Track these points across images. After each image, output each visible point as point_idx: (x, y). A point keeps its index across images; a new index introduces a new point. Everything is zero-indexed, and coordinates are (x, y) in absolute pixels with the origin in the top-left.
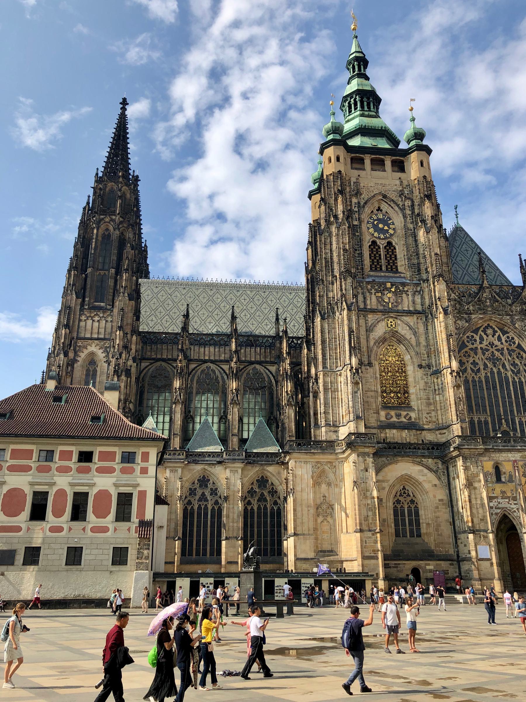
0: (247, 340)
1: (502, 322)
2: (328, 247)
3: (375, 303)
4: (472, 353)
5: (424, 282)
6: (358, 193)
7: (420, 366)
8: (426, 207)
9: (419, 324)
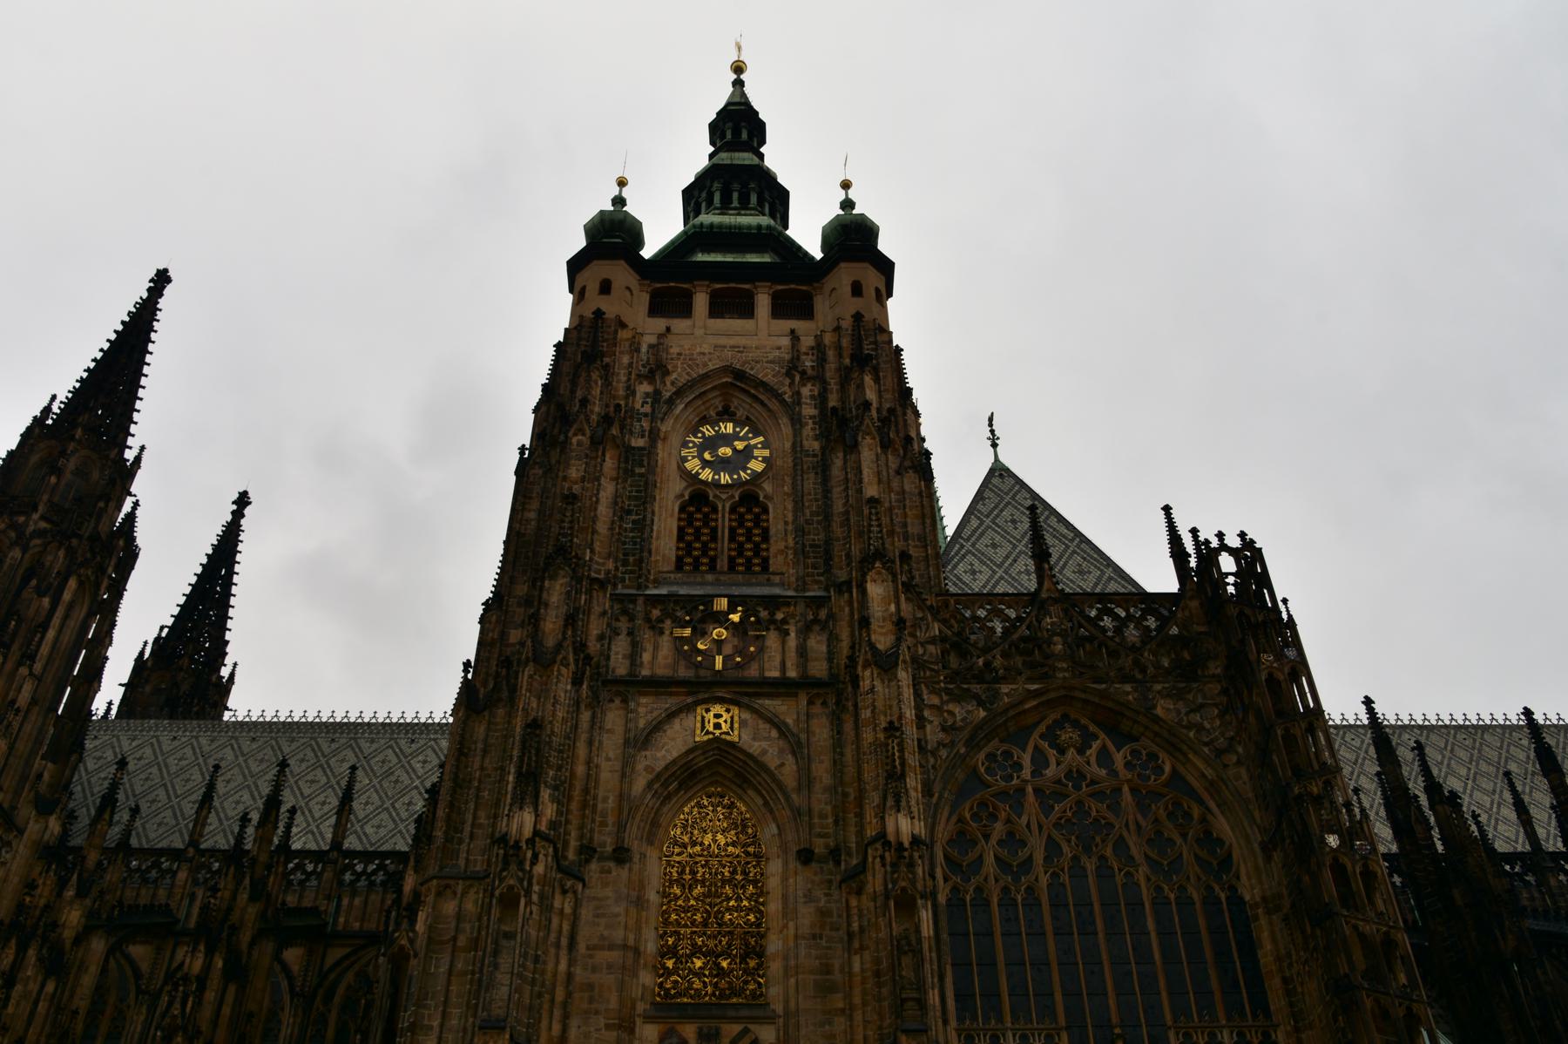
0: (381, 867)
1: (1110, 705)
2: (535, 505)
3: (669, 661)
4: (1004, 811)
5: (840, 592)
6: (657, 369)
7: (806, 856)
8: (853, 386)
9: (815, 721)
